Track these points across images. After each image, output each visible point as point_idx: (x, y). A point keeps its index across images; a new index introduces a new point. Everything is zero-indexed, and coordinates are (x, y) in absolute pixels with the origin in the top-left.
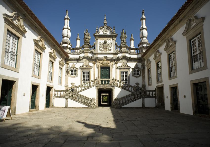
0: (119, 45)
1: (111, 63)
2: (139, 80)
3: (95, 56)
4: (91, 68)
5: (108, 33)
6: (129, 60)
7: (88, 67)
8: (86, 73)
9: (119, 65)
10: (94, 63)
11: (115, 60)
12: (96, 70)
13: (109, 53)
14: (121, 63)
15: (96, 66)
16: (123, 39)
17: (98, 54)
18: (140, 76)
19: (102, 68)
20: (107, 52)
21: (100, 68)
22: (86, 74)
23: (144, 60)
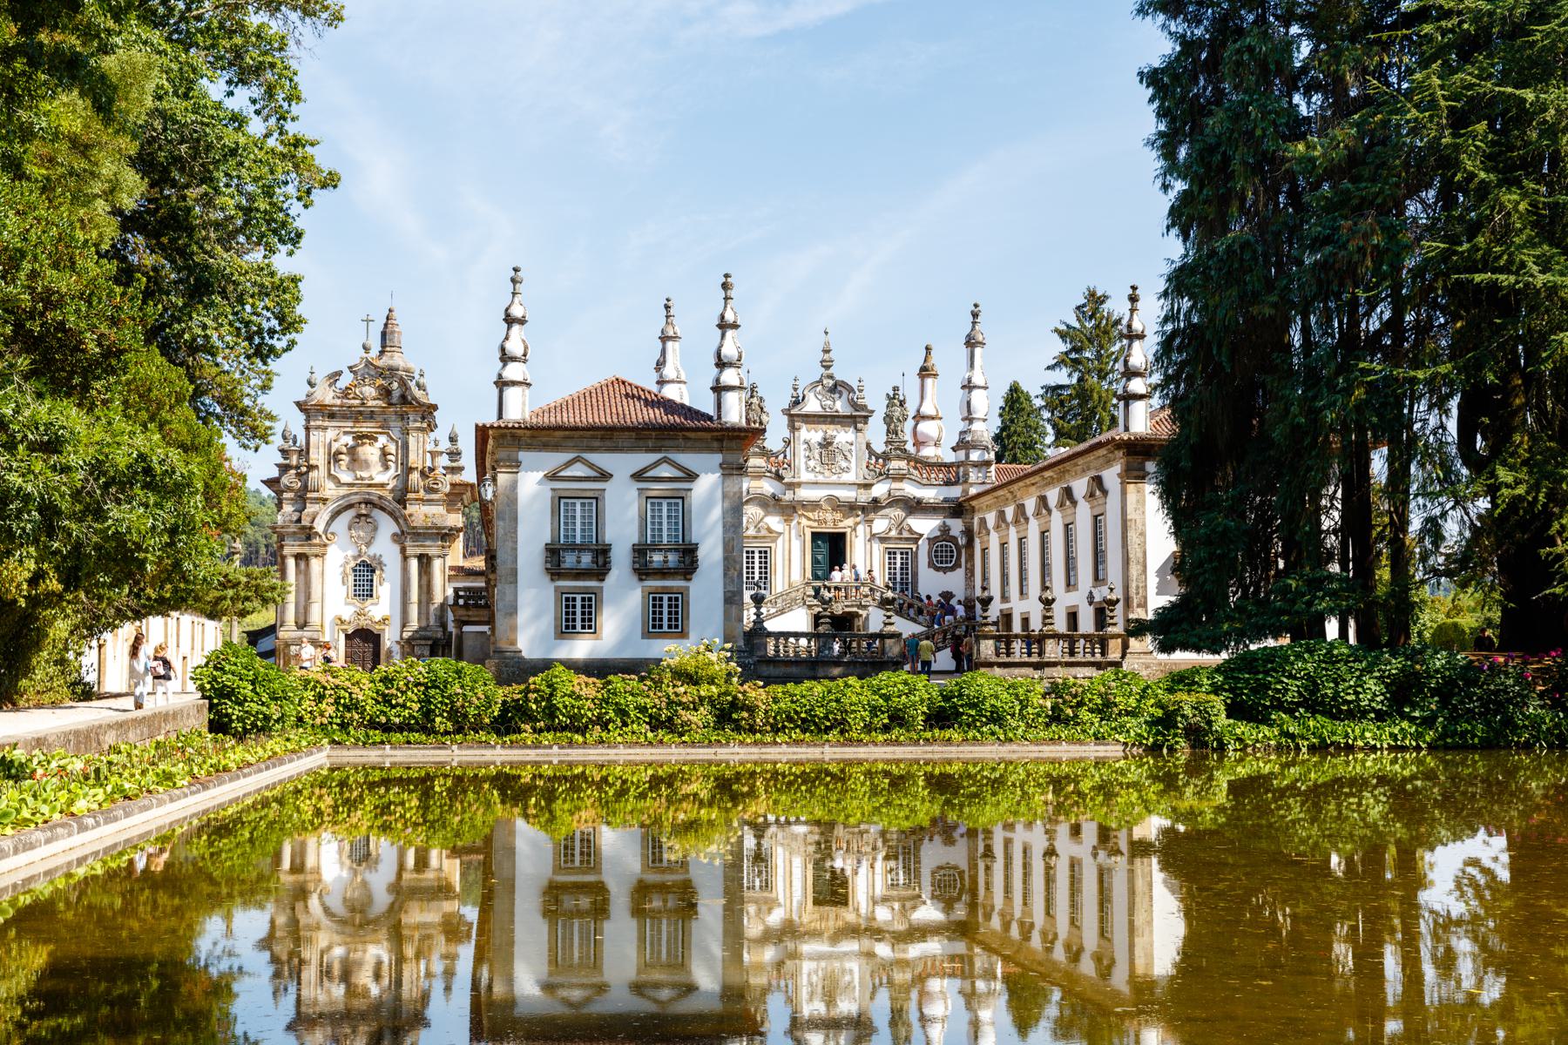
0: (879, 447)
1: (850, 522)
2: (954, 582)
3: (789, 496)
4: (773, 535)
5: (841, 406)
6: (915, 507)
7: (764, 533)
8: (757, 555)
9: (880, 525)
10: (788, 521)
11: (863, 509)
12: (796, 545)
13: (842, 481)
14: (887, 521)
15: (793, 532)
16: (892, 426)
17: (799, 485)
18: (957, 565)
19: (816, 536)
20: (834, 478)
21: (808, 537)
22: (757, 560)
23: (973, 510)
